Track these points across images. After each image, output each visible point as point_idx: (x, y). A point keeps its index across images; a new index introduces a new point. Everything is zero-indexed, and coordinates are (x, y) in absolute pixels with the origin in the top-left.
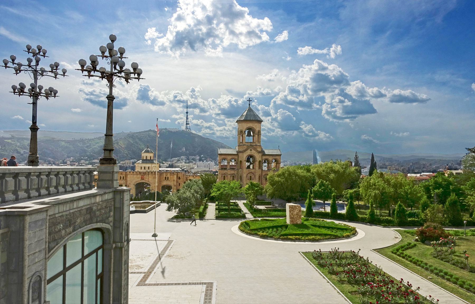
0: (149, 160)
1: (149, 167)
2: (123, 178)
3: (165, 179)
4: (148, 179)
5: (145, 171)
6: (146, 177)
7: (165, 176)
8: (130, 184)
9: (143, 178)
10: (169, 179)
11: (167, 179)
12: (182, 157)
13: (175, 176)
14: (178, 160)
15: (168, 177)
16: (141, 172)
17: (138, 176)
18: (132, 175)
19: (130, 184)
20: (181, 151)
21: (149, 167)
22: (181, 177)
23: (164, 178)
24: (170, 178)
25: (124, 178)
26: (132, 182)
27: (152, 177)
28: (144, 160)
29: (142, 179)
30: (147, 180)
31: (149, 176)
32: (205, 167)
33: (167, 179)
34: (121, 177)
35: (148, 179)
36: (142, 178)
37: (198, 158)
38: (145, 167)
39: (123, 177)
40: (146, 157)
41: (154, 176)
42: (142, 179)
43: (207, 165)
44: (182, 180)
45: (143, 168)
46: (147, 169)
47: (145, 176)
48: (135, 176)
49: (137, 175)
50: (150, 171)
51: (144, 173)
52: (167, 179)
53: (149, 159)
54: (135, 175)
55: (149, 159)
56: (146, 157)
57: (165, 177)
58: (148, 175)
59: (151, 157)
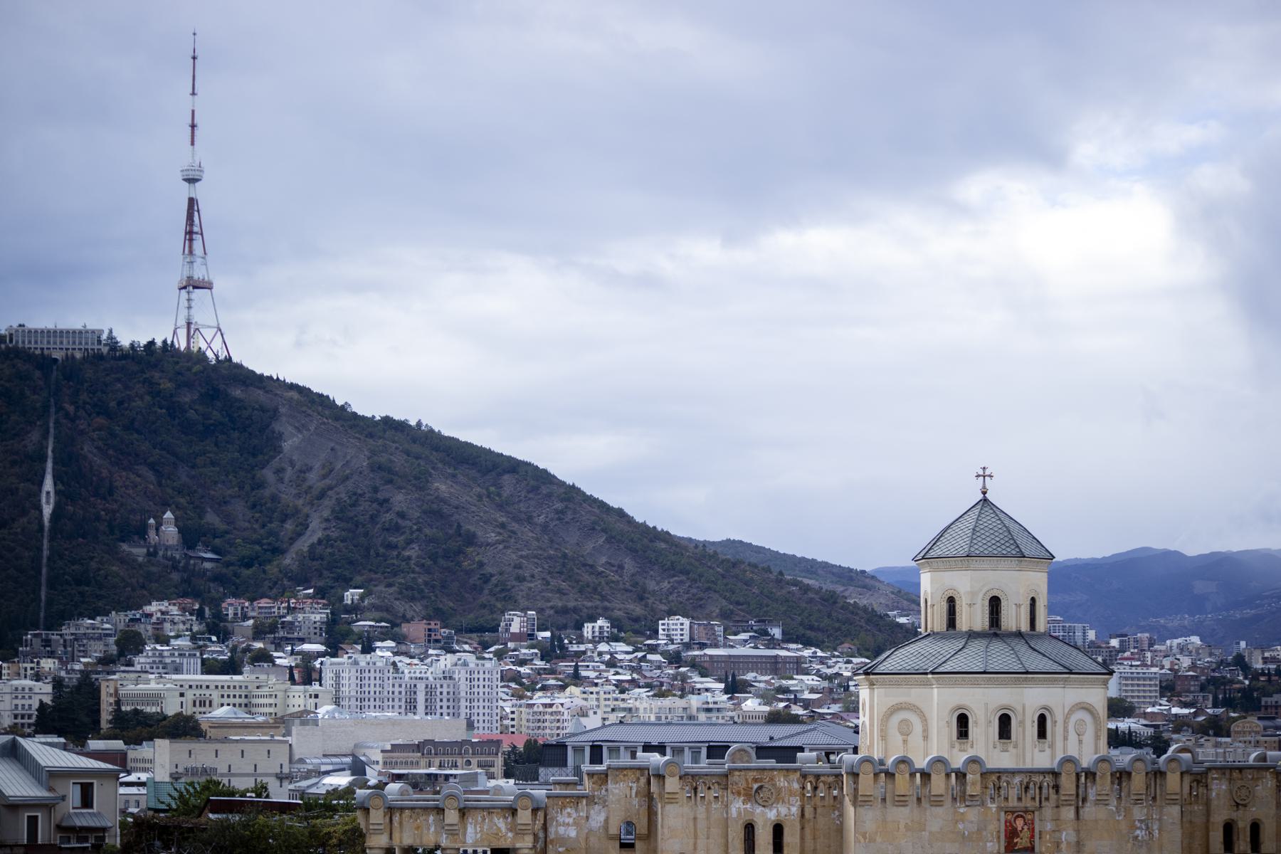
0: (1019, 634)
1: (1042, 720)
5: (1001, 759)
7: (1220, 817)
12: (154, 607)
14: (130, 645)
15: (1255, 828)
16: (1000, 773)
17: (972, 815)
18: (901, 801)
20: (139, 552)
21: (1042, 720)
28: (972, 635)
31: (1089, 811)
32: (411, 706)
37: (317, 616)
38: (1005, 721)
39: (778, 830)
40: (995, 603)
43: (430, 691)
46: (1025, 729)
47: (1048, 811)
48: (937, 818)
49: (961, 797)
53: (1025, 627)
54: (937, 802)
55: (1025, 627)
56: (995, 603)
57: (1229, 828)
58: (1080, 800)
59: (1033, 600)
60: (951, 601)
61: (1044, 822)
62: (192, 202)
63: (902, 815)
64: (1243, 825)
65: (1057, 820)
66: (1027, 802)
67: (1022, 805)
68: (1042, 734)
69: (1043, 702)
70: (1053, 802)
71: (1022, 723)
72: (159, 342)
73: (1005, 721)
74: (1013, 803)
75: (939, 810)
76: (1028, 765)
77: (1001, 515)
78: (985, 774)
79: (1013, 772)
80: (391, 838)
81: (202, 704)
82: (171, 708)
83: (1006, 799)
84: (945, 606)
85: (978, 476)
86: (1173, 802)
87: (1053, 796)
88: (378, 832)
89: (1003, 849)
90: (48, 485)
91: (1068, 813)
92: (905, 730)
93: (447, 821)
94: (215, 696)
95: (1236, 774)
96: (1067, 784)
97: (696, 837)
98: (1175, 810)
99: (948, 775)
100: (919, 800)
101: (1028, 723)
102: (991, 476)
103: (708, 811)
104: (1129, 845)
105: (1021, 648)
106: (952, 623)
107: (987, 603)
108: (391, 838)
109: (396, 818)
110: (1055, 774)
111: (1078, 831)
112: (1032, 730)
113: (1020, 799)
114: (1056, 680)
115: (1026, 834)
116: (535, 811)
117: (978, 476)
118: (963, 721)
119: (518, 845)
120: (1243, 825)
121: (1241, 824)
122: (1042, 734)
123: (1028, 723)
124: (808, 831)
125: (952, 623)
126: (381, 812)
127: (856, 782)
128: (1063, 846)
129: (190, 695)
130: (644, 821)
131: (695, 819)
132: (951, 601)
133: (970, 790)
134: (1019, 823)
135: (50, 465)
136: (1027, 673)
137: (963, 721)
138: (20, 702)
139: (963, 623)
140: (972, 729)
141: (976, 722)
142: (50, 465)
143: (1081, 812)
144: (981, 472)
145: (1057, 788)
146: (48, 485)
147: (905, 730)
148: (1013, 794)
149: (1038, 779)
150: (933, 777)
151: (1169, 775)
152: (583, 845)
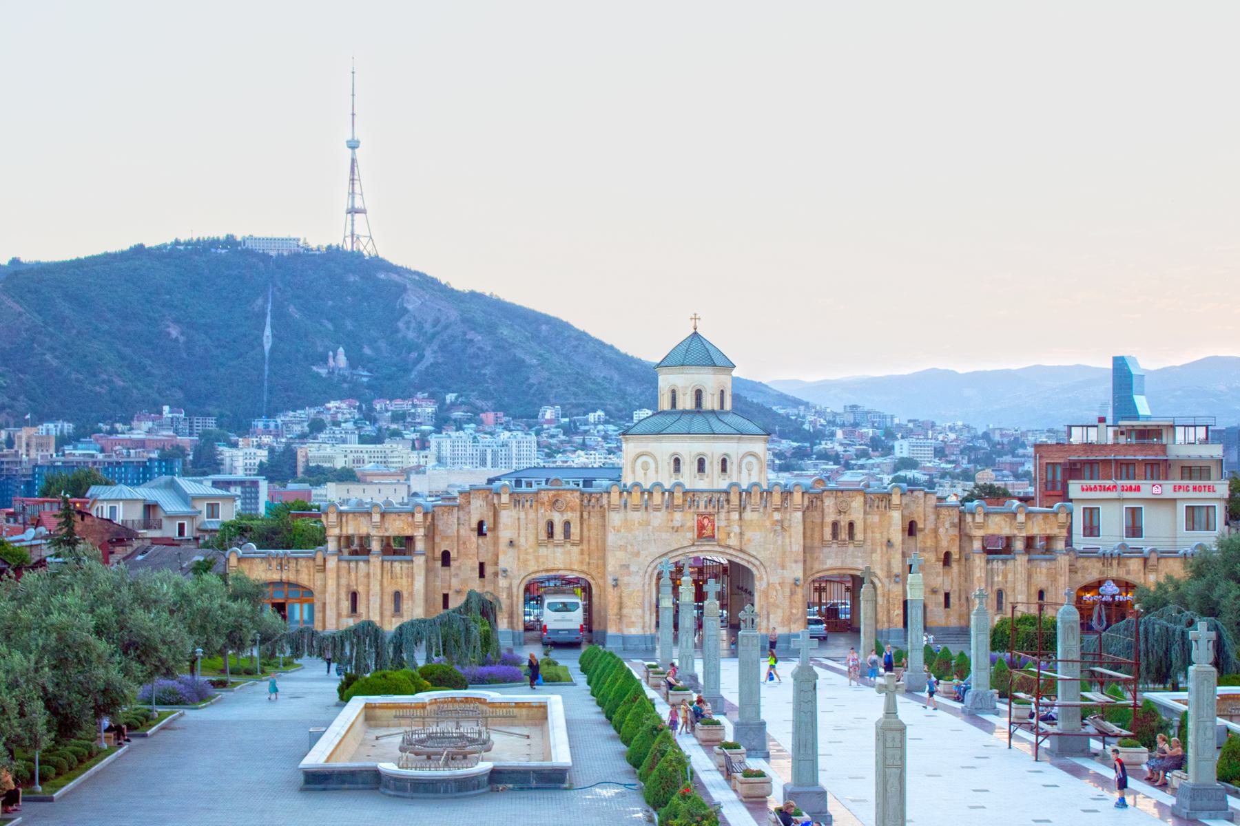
0: (713, 412)
1: (724, 461)
2: (567, 534)
3: (835, 535)
5: (702, 484)
6: (727, 522)
7: (830, 519)
8: (627, 566)
9: (707, 532)
10: (859, 536)
11: (844, 535)
12: (332, 405)
13: (896, 515)
14: (317, 427)
15: (851, 525)
16: (694, 492)
17: (678, 516)
18: (636, 508)
19: (627, 566)
20: (323, 372)
21: (724, 461)
22: (920, 525)
23: (828, 531)
24: (865, 530)
25: (575, 530)
26: (638, 554)
27: (768, 524)
28: (684, 412)
29: (704, 533)
30: (733, 541)
31: (748, 515)
32: (483, 463)
33: (845, 532)
34: (551, 525)
36: (701, 527)
37: (430, 409)
38: (701, 463)
39: (567, 524)
40: (699, 394)
41: (777, 516)
42: (700, 536)
43: (494, 453)
44: (929, 543)
45: (689, 468)
46: (713, 467)
47: (723, 515)
48: (658, 518)
49: (671, 507)
50: (733, 485)
51: (721, 498)
52: (844, 535)
53: (717, 407)
54: (657, 509)
55: (717, 407)
56: (699, 394)
57: (835, 525)
58: (742, 509)
59: (722, 391)
60: (674, 392)
61: (720, 521)
62: (353, 161)
63: (637, 516)
64: (844, 523)
65: (728, 519)
66: (710, 510)
67: (708, 510)
68: (724, 470)
69: (725, 451)
70: (725, 510)
71: (711, 463)
72: (201, 239)
73: (701, 463)
74: (702, 509)
75: (658, 514)
76: (715, 487)
77: (705, 342)
78: (685, 493)
79: (702, 492)
80: (341, 530)
81: (358, 462)
82: (339, 464)
83: (698, 507)
84: (670, 395)
85: (691, 319)
86: (797, 510)
87: (726, 506)
88: (333, 527)
89: (696, 537)
90: (268, 332)
91: (735, 516)
92: (645, 467)
93: (374, 520)
94: (366, 456)
95: (840, 494)
96: (734, 499)
97: (519, 529)
98: (799, 515)
99: (663, 493)
100: (646, 508)
101: (715, 463)
102: (699, 319)
103: (526, 514)
104: (772, 535)
105: (713, 420)
106: (674, 405)
107: (694, 393)
108: (341, 530)
109: (344, 519)
110: (727, 493)
111: (741, 526)
112: (718, 467)
113: (706, 507)
114: (732, 438)
115: (710, 527)
116: (425, 514)
117: (691, 319)
118: (677, 461)
119: (415, 534)
120: (844, 523)
121: (842, 524)
122: (724, 470)
123: (715, 463)
124: (585, 526)
125: (674, 405)
126: (335, 515)
127: (609, 497)
128: (732, 535)
129: (351, 456)
130: (491, 520)
131: (519, 519)
132: (674, 392)
133: (676, 502)
134: (706, 522)
135: (268, 320)
136: (714, 434)
137: (677, 461)
138: (248, 461)
139: (680, 406)
140: (683, 468)
141: (684, 463)
142: (268, 320)
143: (743, 515)
144: (693, 317)
145: (728, 501)
146: (268, 332)
147: (645, 467)
148: (702, 504)
149: (716, 496)
150: (655, 494)
151: (795, 494)
152: (456, 534)
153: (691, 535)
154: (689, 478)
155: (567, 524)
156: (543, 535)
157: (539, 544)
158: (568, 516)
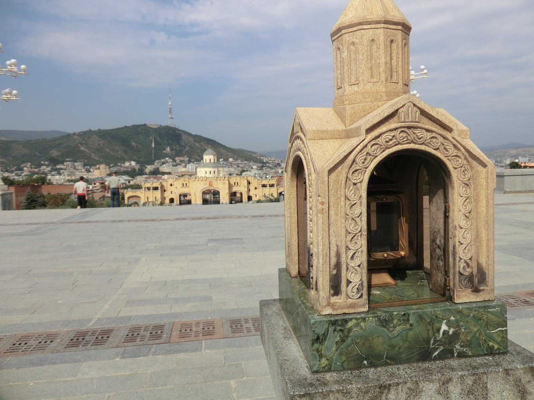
4: (217, 185)
5: (211, 176)
9: (211, 185)
25: (187, 185)
29: (210, 185)
34: (183, 184)
35: (217, 185)
36: (210, 184)
39: (186, 184)
42: (210, 185)
45: (208, 173)
118: (206, 172)
137: (206, 172)
140: (207, 173)
153: (208, 185)
154: (208, 175)
155: (186, 184)
156: (182, 186)
157: (182, 187)
158: (186, 182)
